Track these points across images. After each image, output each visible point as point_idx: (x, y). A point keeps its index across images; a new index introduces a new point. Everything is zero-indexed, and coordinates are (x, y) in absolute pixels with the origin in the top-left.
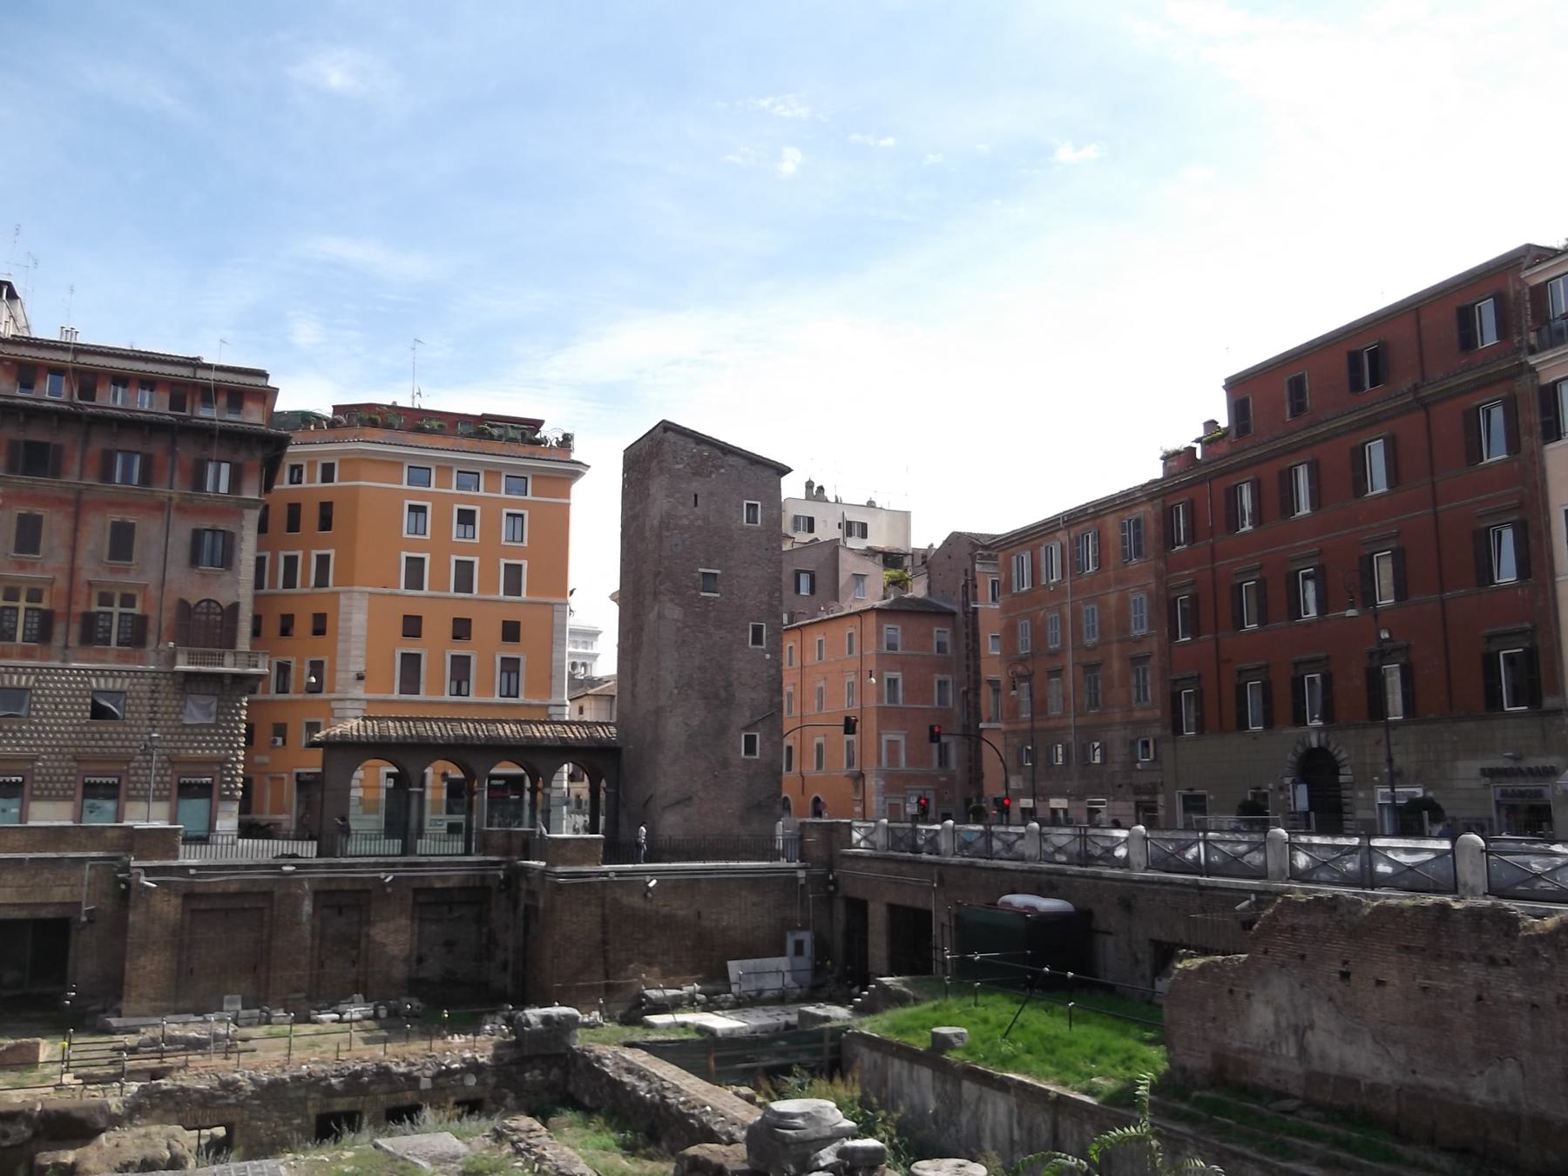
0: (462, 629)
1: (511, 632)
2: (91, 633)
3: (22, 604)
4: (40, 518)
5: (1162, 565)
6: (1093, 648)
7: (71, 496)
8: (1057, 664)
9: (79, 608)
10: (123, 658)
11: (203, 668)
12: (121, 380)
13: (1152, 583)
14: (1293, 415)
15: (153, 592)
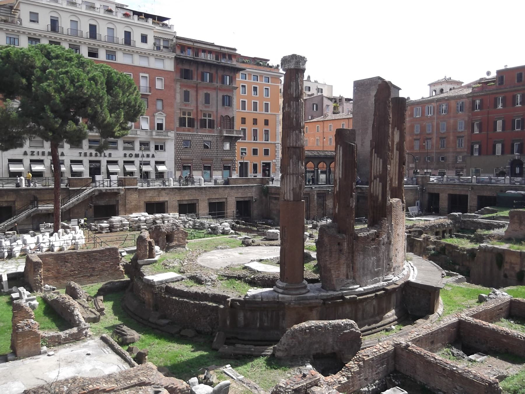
0: (255, 121)
1: (266, 122)
2: (203, 124)
3: (187, 116)
4: (189, 92)
5: (470, 114)
6: (444, 133)
7: (195, 85)
8: (430, 137)
9: (199, 118)
10: (210, 132)
11: (230, 135)
12: (204, 51)
13: (466, 118)
14: (518, 81)
15: (215, 113)
